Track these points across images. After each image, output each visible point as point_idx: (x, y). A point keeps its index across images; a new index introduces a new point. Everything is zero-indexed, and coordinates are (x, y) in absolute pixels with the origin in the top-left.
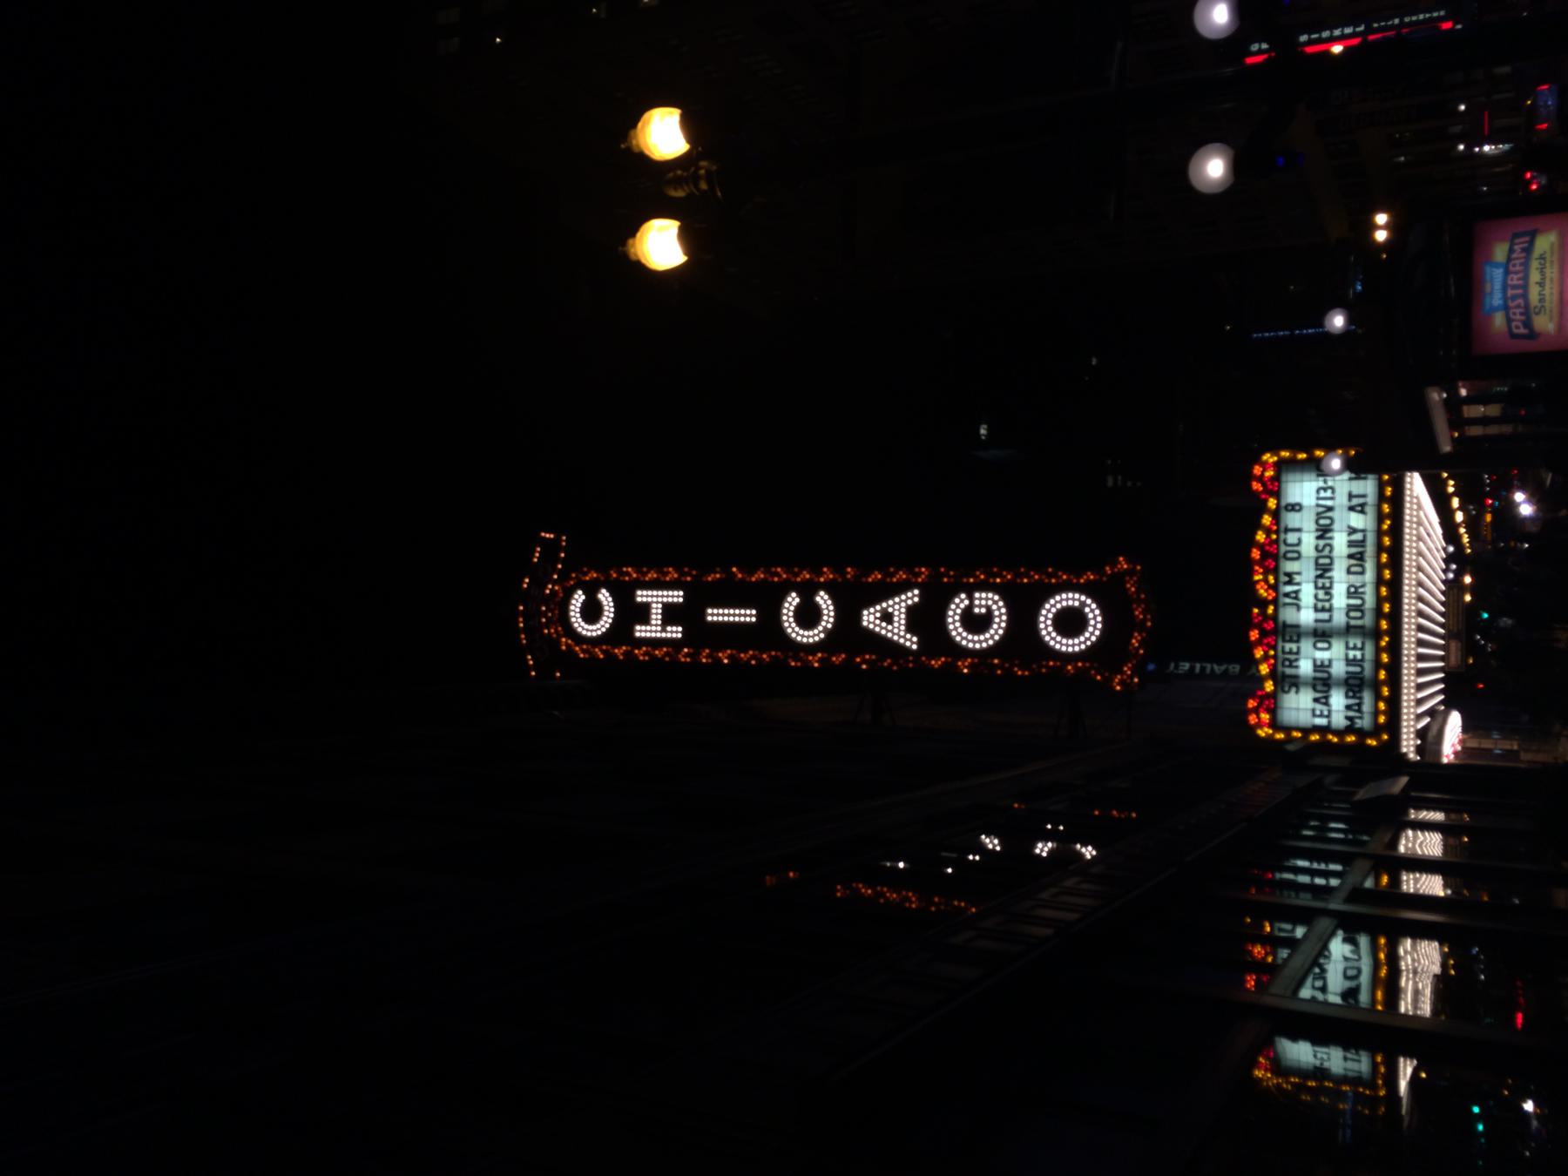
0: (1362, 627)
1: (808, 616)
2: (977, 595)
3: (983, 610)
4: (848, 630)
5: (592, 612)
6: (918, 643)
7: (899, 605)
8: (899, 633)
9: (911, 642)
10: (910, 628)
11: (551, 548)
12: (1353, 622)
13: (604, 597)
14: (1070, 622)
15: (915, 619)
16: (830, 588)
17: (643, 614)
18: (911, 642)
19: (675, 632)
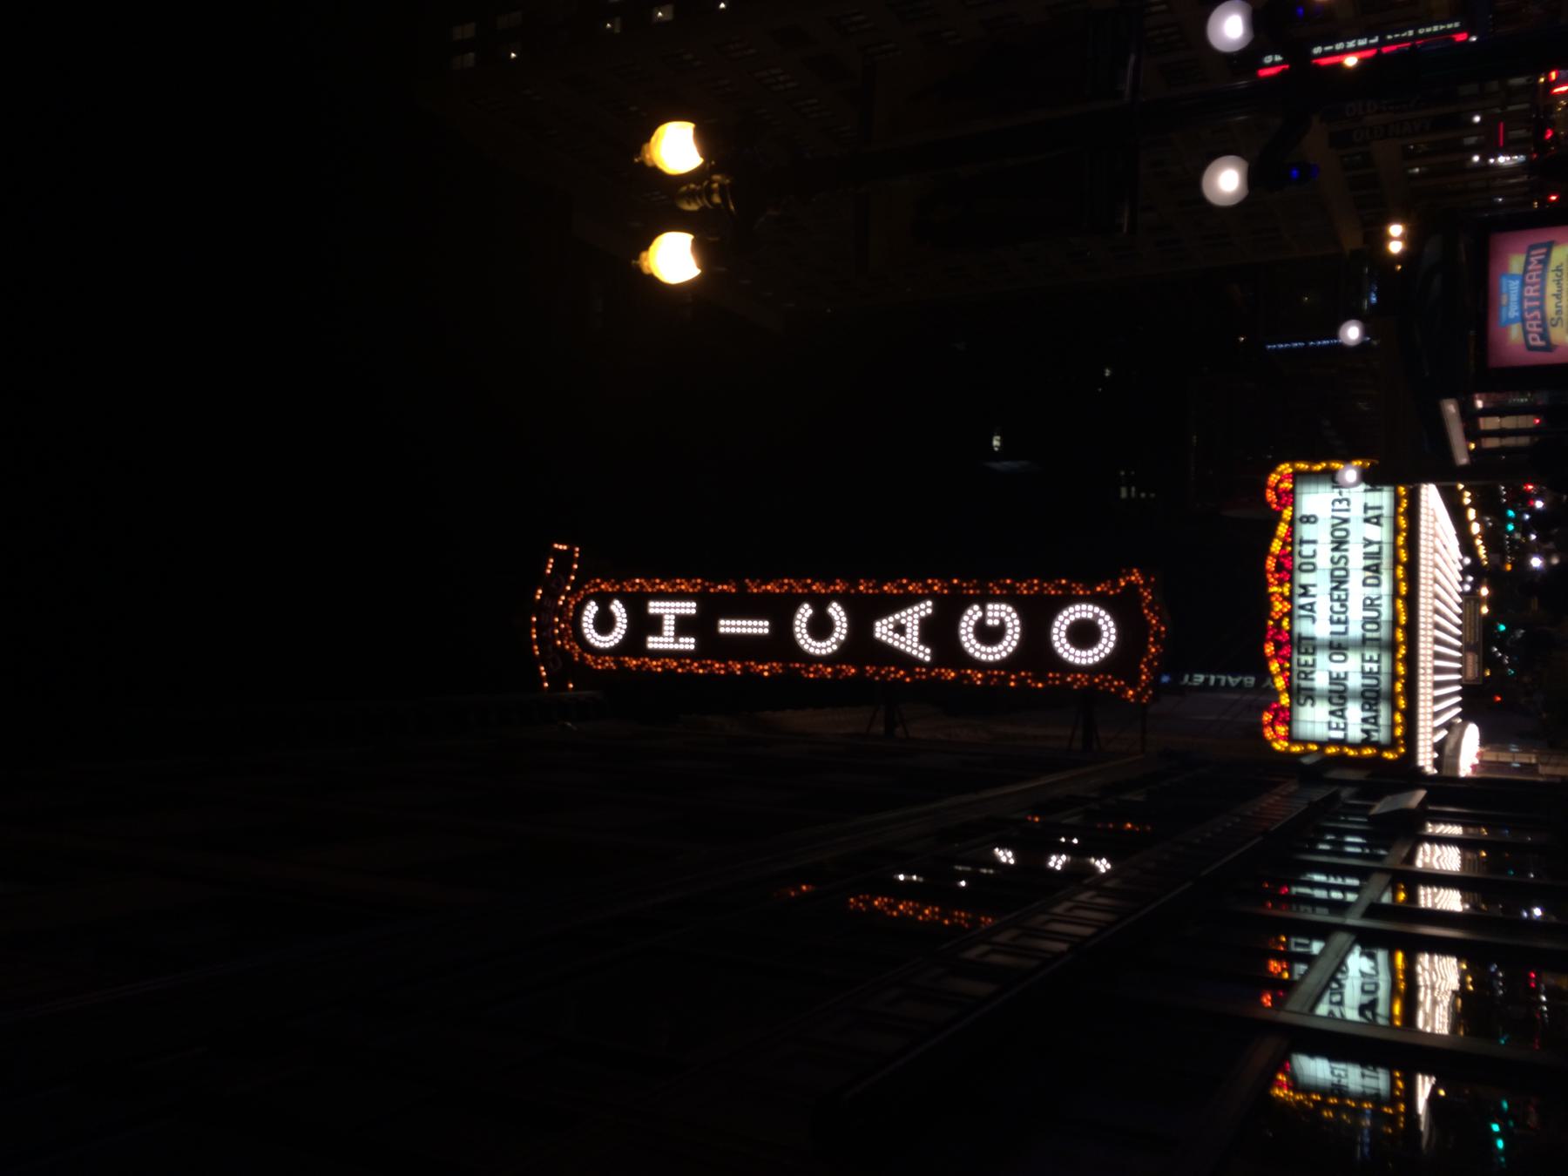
0: (1378, 640)
1: (821, 627)
2: (990, 606)
3: (997, 622)
4: (861, 643)
5: (604, 623)
6: (932, 655)
7: (913, 616)
8: (912, 644)
9: (924, 654)
10: (924, 638)
11: (564, 560)
12: (1369, 635)
13: (617, 608)
14: (1084, 634)
15: (928, 631)
16: (844, 601)
17: (655, 625)
18: (924, 654)
19: (688, 643)
